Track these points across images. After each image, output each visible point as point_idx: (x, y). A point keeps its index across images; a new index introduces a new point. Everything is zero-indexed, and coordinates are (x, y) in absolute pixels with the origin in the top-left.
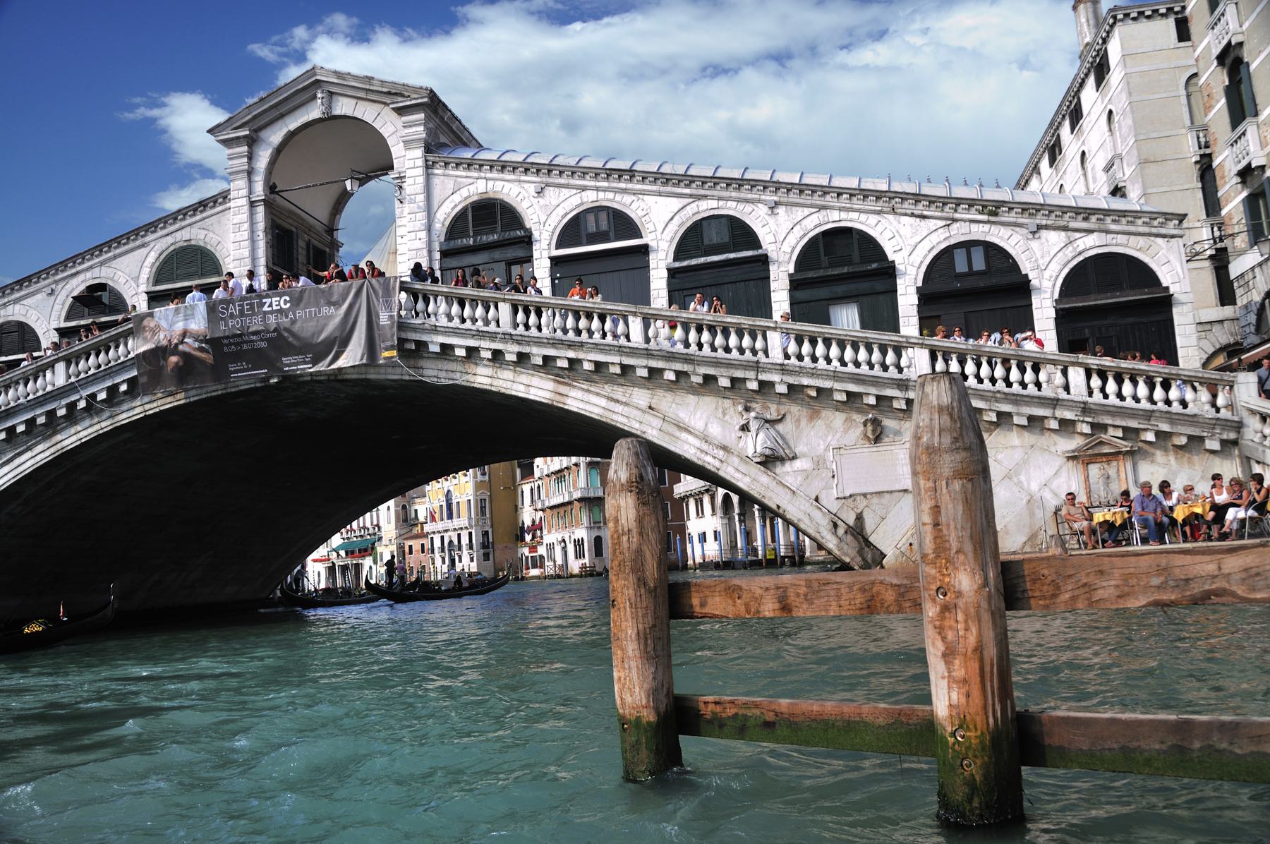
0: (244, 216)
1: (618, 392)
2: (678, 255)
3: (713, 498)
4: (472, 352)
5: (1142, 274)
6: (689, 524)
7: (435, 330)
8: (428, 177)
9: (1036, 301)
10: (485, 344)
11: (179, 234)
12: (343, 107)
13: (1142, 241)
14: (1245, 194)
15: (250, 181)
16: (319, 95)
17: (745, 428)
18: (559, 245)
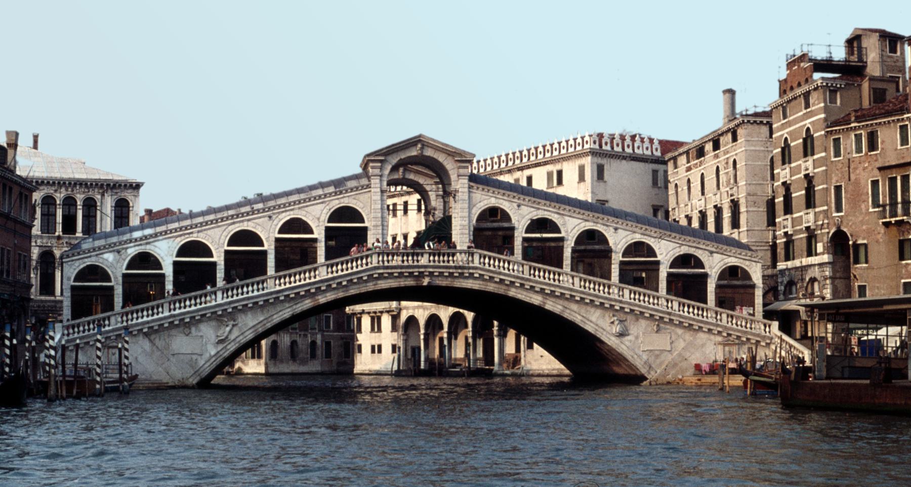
0: (379, 198)
1: (566, 303)
2: (577, 243)
3: (395, 318)
4: (512, 283)
5: (747, 276)
6: (358, 335)
7: (500, 273)
8: (470, 192)
9: (709, 281)
10: (519, 281)
11: (342, 200)
12: (429, 152)
13: (747, 263)
14: (785, 240)
15: (381, 180)
16: (419, 146)
17: (613, 323)
18: (527, 232)
